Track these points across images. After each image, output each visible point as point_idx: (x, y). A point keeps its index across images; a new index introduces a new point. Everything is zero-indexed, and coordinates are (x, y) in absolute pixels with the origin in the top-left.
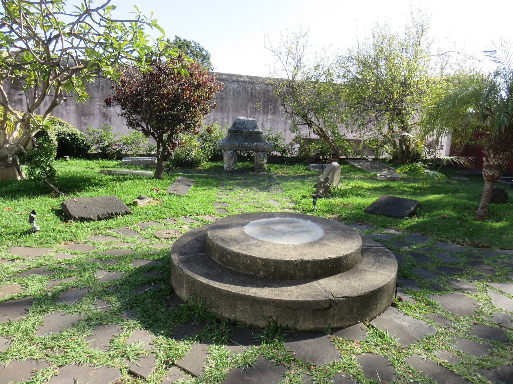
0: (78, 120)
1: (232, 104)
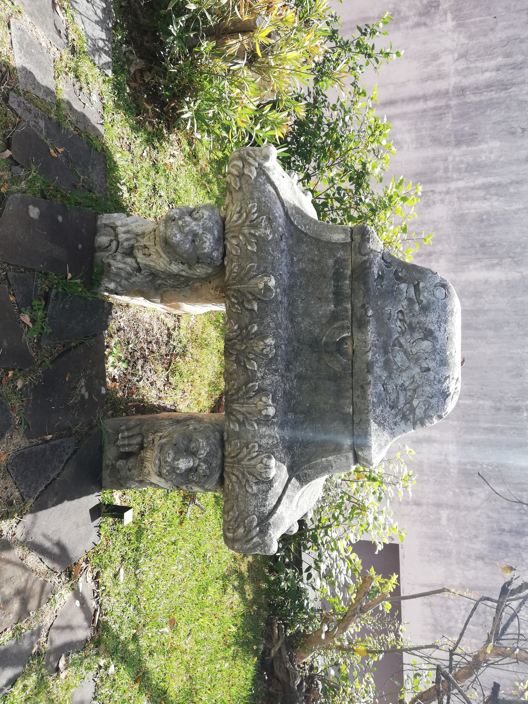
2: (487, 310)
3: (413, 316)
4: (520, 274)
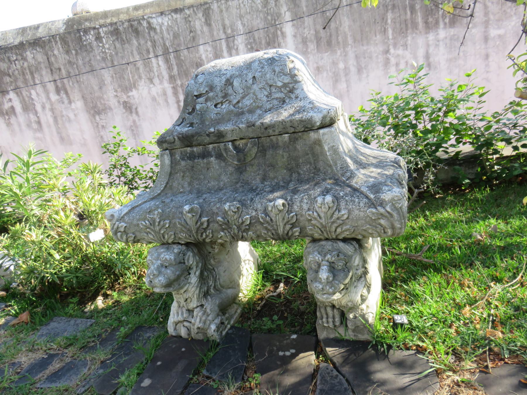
0: (92, 122)
1: (350, 27)
2: (316, 31)
3: (217, 96)
4: (287, 13)
